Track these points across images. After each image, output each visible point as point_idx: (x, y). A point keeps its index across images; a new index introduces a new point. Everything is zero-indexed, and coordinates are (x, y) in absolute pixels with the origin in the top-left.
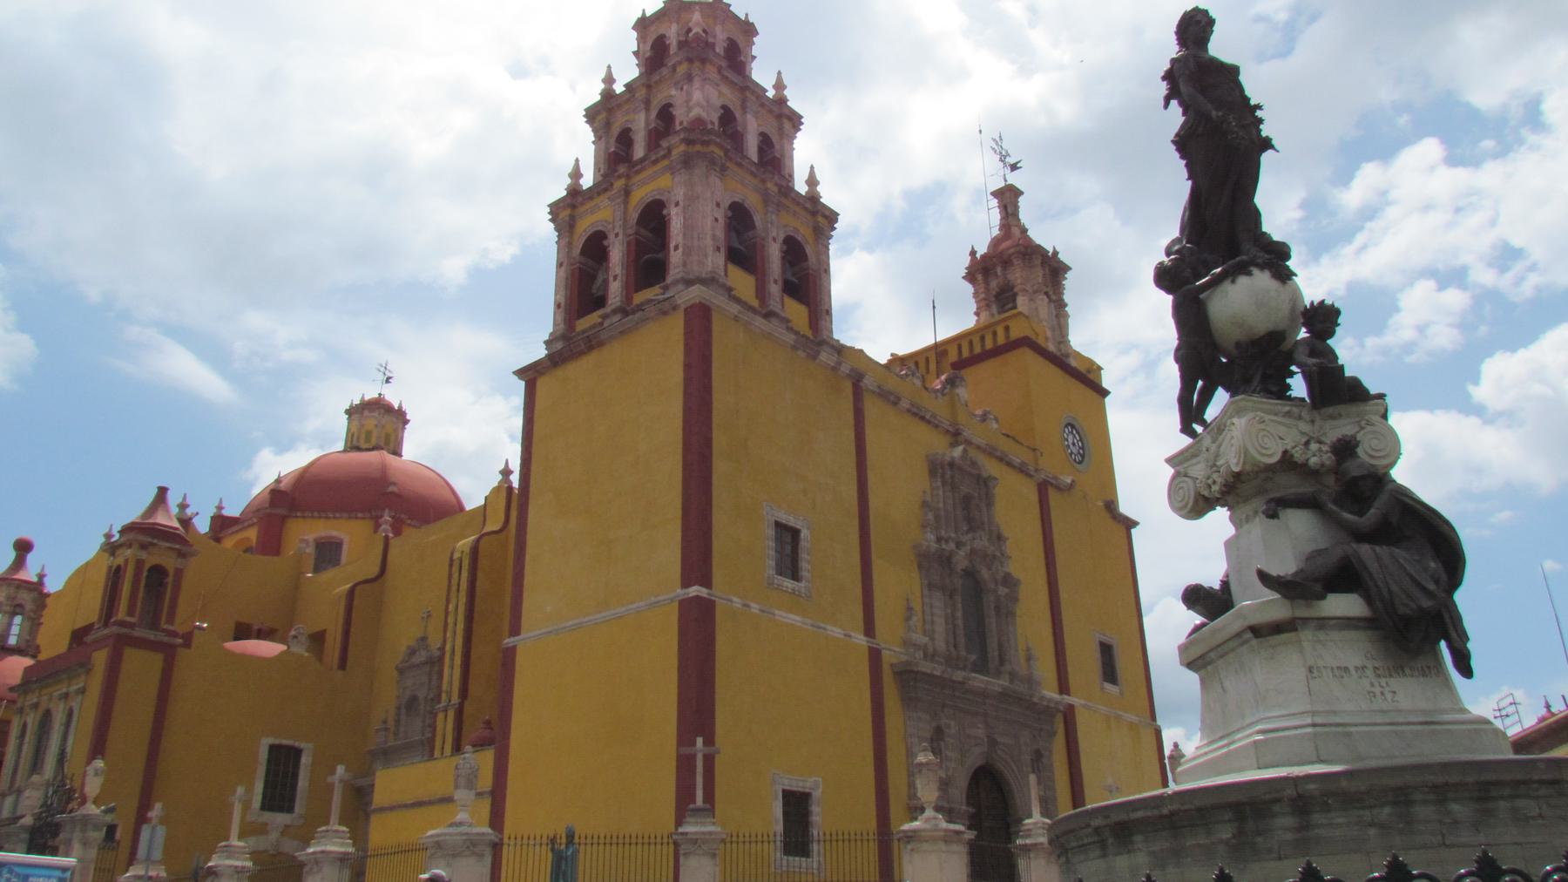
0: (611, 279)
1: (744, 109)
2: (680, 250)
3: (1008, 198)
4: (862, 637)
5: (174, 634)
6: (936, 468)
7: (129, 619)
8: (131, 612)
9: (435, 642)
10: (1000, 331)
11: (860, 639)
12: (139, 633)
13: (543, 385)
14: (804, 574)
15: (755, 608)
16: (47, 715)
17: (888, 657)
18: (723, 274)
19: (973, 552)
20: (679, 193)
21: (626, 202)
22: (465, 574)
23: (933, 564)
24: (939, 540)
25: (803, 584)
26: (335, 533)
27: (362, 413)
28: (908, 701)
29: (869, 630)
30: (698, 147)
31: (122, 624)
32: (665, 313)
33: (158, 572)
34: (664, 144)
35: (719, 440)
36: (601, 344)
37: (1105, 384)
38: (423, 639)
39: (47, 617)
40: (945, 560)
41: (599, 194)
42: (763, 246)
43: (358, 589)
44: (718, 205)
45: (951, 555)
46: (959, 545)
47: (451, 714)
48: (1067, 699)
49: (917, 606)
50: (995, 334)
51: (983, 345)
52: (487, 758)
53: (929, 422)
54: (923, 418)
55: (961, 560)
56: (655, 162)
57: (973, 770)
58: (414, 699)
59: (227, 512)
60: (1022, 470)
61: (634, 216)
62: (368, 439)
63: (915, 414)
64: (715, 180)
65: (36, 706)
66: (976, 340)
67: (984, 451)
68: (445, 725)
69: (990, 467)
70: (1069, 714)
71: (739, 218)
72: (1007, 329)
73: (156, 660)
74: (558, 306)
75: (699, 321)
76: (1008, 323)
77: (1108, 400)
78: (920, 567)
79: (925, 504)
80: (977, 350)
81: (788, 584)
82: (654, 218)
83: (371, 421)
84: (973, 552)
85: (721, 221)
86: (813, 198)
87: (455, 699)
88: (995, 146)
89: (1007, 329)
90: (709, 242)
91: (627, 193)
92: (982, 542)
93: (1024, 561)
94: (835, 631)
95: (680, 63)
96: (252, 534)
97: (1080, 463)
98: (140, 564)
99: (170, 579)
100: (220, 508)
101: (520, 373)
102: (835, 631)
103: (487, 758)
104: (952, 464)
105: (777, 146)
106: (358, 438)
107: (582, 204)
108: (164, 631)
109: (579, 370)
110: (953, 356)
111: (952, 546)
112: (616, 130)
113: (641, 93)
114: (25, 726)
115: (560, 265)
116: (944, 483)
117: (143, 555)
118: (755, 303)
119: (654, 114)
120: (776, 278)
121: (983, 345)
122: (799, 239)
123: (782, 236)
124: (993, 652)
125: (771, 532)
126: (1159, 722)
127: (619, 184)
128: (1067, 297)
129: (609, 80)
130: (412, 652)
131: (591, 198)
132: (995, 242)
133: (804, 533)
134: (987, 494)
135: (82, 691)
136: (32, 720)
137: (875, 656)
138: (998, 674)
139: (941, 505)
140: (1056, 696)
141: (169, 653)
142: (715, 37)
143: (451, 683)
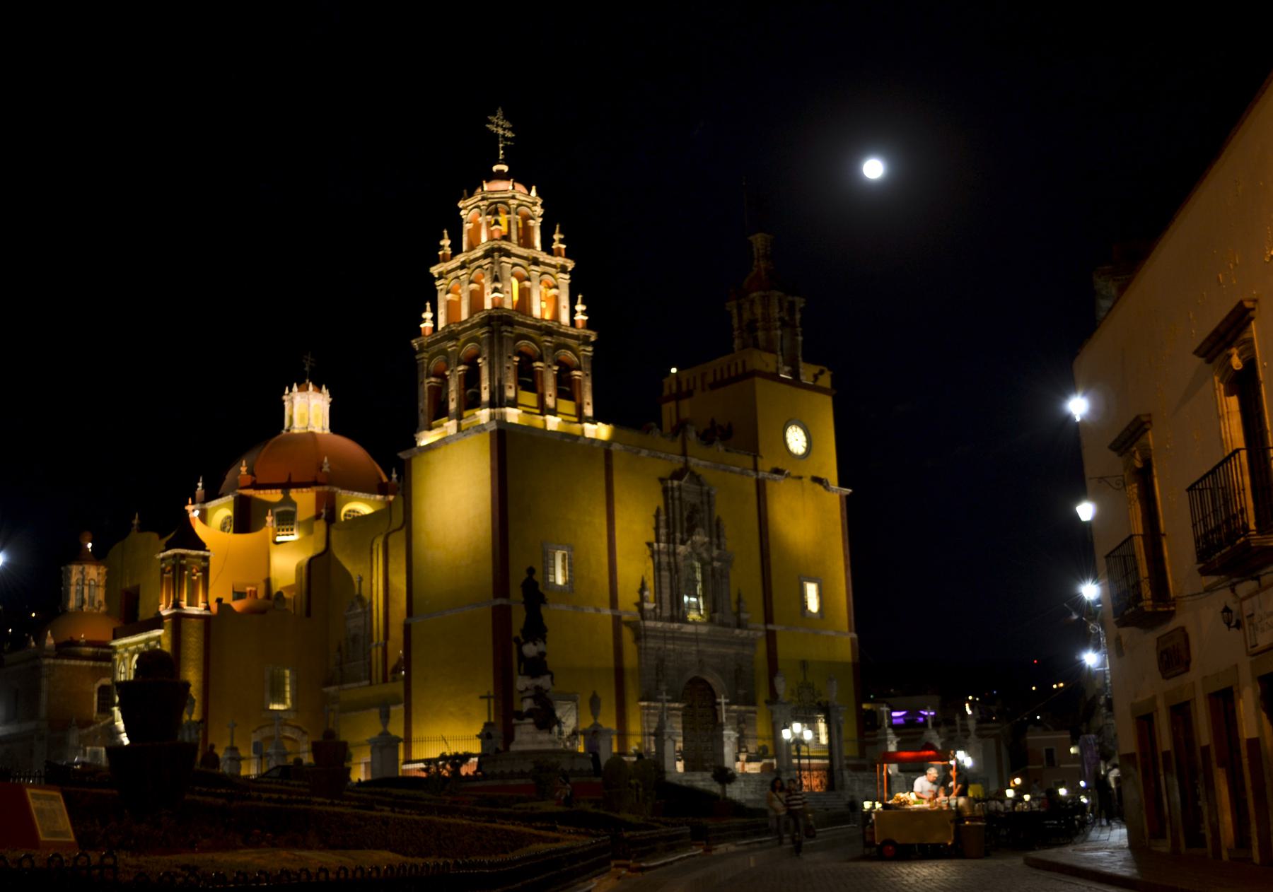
0: (450, 400)
2: (488, 390)
11: (607, 612)
36: (447, 443)
47: (380, 649)
48: (770, 627)
49: (650, 584)
50: (736, 364)
53: (664, 459)
54: (660, 458)
60: (743, 473)
63: (653, 457)
70: (771, 637)
72: (744, 363)
78: (652, 556)
84: (692, 542)
85: (512, 368)
89: (744, 363)
93: (740, 540)
120: (550, 393)
134: (709, 502)
139: (671, 515)
140: (762, 627)
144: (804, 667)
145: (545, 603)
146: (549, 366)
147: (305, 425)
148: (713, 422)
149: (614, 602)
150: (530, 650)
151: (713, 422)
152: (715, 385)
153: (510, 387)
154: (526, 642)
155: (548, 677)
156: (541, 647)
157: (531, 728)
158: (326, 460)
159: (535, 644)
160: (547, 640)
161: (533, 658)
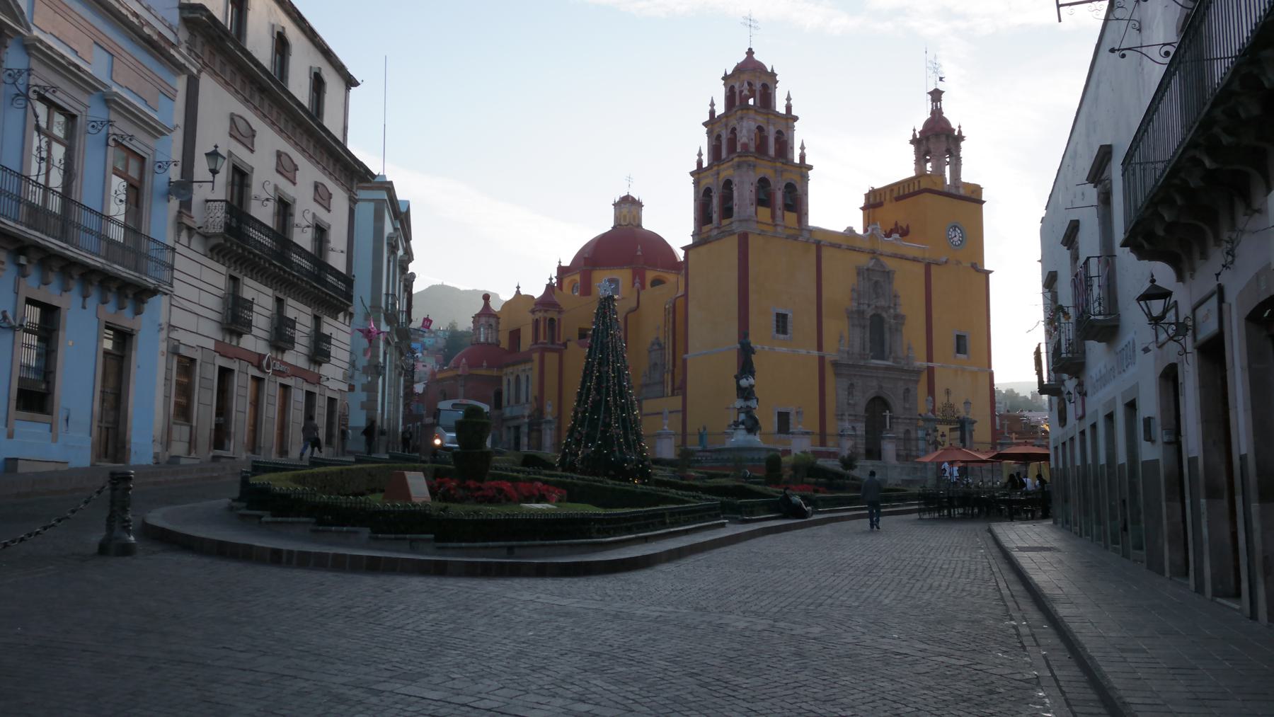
1: (768, 123)
3: (936, 95)
4: (816, 352)
5: (560, 345)
6: (860, 272)
7: (545, 341)
8: (545, 339)
9: (662, 341)
10: (916, 184)
11: (815, 353)
12: (549, 346)
13: (690, 252)
14: (789, 331)
15: (766, 348)
16: (518, 376)
17: (828, 358)
18: (754, 214)
19: (876, 307)
20: (736, 180)
21: (718, 178)
22: (671, 315)
23: (855, 316)
24: (859, 304)
25: (788, 336)
26: (614, 277)
27: (620, 206)
28: (837, 375)
29: (820, 348)
30: (744, 159)
31: (542, 343)
32: (731, 235)
33: (552, 320)
34: (731, 157)
35: (752, 286)
36: (710, 242)
37: (983, 199)
38: (657, 338)
39: (501, 327)
40: (861, 313)
41: (709, 170)
42: (774, 193)
43: (629, 315)
44: (752, 184)
45: (863, 312)
46: (869, 305)
48: (930, 364)
50: (914, 183)
51: (909, 189)
52: (680, 398)
53: (858, 251)
54: (855, 250)
55: (870, 312)
56: (728, 162)
57: (868, 400)
58: (656, 364)
59: (562, 264)
60: (915, 260)
61: (721, 184)
62: (625, 220)
63: (850, 250)
64: (751, 173)
65: (512, 373)
66: (906, 185)
67: (891, 256)
68: (668, 377)
69: (890, 264)
70: (931, 371)
71: (763, 182)
72: (919, 182)
73: (555, 356)
74: (695, 219)
75: (744, 240)
76: (919, 179)
77: (984, 205)
78: (848, 317)
79: (853, 290)
80: (906, 192)
81: (782, 336)
82: (728, 184)
83: (626, 209)
84: (876, 307)
85: (754, 191)
86: (802, 157)
87: (671, 368)
88: (929, 65)
90: (748, 201)
91: (718, 174)
92: (882, 303)
94: (803, 352)
95: (738, 110)
96: (577, 277)
97: (959, 245)
98: (545, 319)
99: (557, 322)
100: (560, 262)
101: (683, 248)
102: (803, 352)
103: (677, 402)
104: (868, 269)
105: (785, 135)
106: (620, 219)
107: (702, 173)
108: (558, 344)
109: (703, 249)
110: (895, 194)
111: (866, 307)
112: (715, 134)
113: (724, 120)
114: (509, 380)
115: (695, 200)
116: (864, 279)
117: (545, 315)
118: (770, 221)
119: (729, 130)
121: (909, 189)
122: (793, 182)
123: (784, 184)
124: (887, 350)
125: (775, 318)
126: (993, 368)
127: (715, 168)
128: (962, 154)
129: (712, 104)
130: (653, 344)
131: (705, 171)
132: (928, 124)
133: (790, 315)
135: (531, 369)
136: (512, 379)
137: (822, 359)
138: (887, 360)
141: (560, 352)
142: (755, 86)
143: (669, 360)
144: (948, 393)
145: (754, 353)
146: (779, 189)
147: (626, 224)
148: (896, 224)
149: (820, 348)
150: (744, 383)
151: (896, 224)
152: (898, 199)
153: (752, 204)
154: (743, 378)
155: (755, 401)
156: (752, 381)
157: (744, 432)
158: (639, 247)
159: (747, 380)
160: (755, 377)
161: (746, 388)
